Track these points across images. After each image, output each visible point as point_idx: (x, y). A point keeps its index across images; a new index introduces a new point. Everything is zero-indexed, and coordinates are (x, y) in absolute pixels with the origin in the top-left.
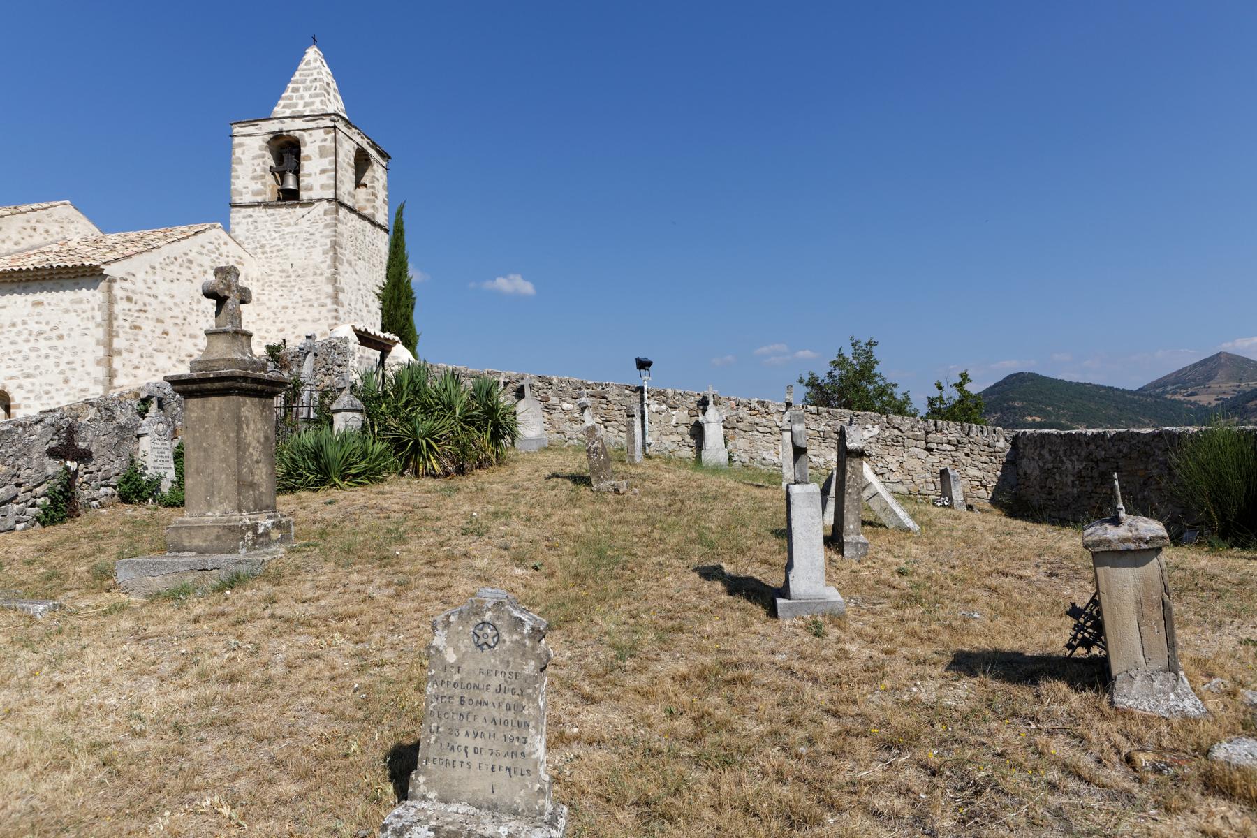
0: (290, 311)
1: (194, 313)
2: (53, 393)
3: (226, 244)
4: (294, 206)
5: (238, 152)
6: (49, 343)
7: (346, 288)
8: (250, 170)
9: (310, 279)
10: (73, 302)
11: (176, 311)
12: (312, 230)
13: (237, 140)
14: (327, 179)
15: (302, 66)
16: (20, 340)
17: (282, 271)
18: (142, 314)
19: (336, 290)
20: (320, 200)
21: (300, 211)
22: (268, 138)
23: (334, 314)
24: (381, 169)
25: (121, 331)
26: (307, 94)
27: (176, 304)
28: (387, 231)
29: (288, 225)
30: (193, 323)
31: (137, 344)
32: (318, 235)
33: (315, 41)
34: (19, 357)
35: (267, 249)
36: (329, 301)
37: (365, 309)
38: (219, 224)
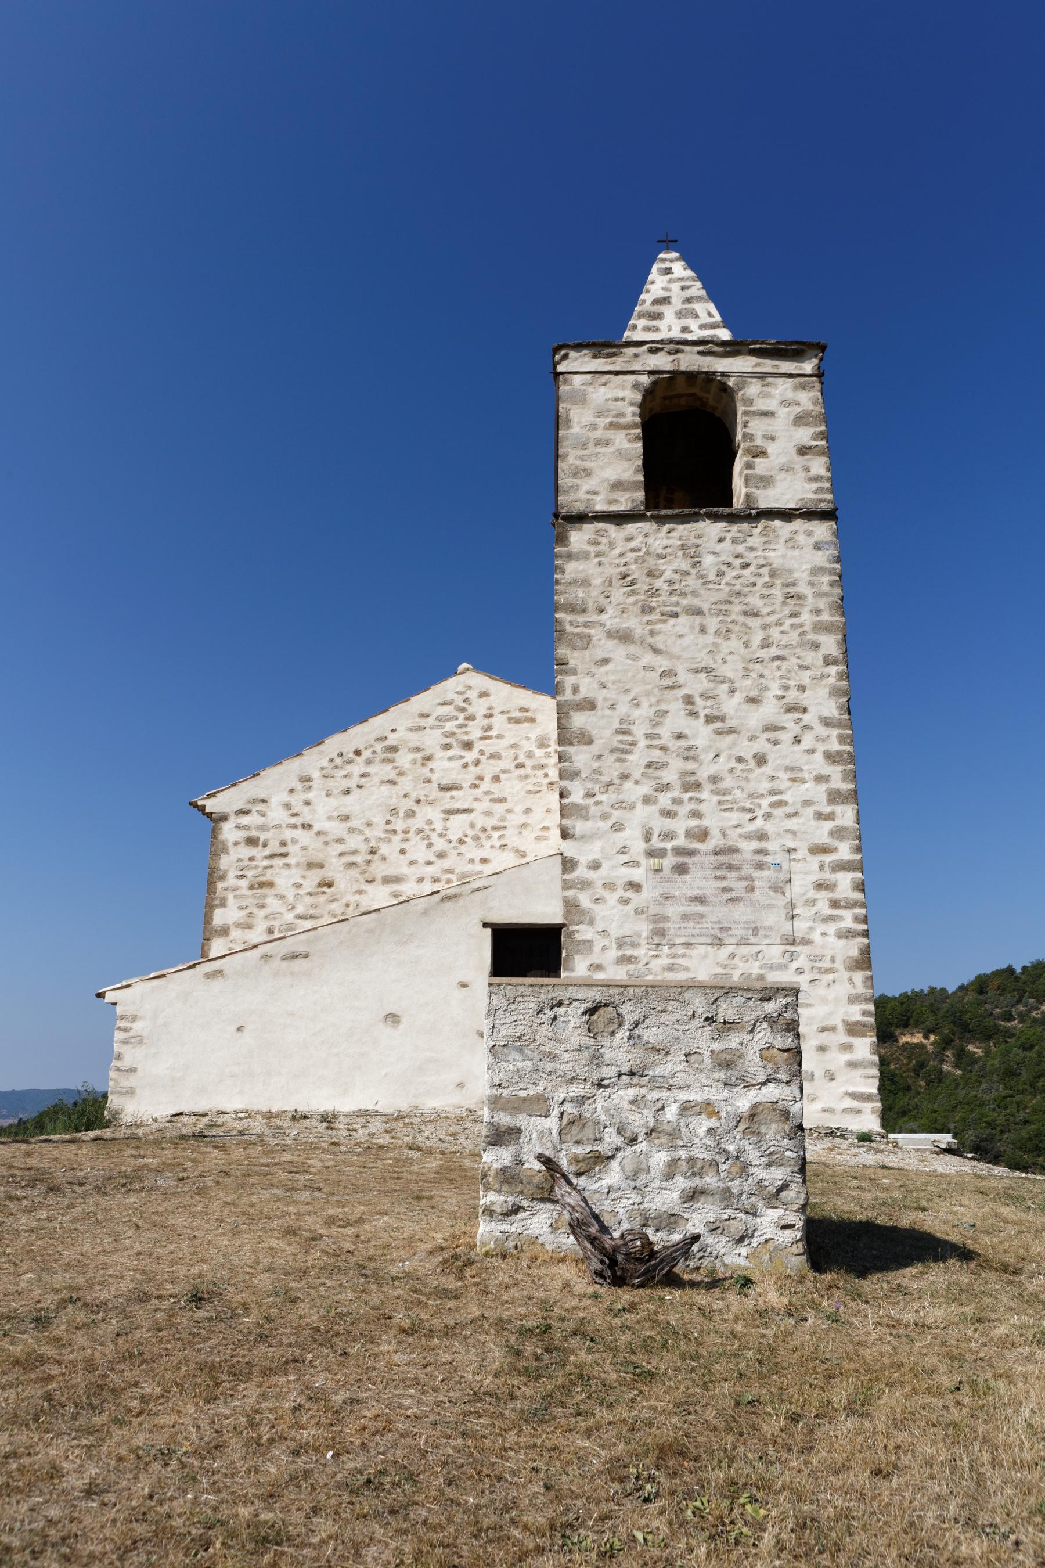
1: (396, 839)
3: (484, 694)
7: (600, 696)
11: (354, 842)
18: (278, 862)
24: (783, 388)
25: (230, 896)
27: (352, 830)
31: (262, 913)
33: (668, 244)
37: (701, 734)
38: (465, 665)
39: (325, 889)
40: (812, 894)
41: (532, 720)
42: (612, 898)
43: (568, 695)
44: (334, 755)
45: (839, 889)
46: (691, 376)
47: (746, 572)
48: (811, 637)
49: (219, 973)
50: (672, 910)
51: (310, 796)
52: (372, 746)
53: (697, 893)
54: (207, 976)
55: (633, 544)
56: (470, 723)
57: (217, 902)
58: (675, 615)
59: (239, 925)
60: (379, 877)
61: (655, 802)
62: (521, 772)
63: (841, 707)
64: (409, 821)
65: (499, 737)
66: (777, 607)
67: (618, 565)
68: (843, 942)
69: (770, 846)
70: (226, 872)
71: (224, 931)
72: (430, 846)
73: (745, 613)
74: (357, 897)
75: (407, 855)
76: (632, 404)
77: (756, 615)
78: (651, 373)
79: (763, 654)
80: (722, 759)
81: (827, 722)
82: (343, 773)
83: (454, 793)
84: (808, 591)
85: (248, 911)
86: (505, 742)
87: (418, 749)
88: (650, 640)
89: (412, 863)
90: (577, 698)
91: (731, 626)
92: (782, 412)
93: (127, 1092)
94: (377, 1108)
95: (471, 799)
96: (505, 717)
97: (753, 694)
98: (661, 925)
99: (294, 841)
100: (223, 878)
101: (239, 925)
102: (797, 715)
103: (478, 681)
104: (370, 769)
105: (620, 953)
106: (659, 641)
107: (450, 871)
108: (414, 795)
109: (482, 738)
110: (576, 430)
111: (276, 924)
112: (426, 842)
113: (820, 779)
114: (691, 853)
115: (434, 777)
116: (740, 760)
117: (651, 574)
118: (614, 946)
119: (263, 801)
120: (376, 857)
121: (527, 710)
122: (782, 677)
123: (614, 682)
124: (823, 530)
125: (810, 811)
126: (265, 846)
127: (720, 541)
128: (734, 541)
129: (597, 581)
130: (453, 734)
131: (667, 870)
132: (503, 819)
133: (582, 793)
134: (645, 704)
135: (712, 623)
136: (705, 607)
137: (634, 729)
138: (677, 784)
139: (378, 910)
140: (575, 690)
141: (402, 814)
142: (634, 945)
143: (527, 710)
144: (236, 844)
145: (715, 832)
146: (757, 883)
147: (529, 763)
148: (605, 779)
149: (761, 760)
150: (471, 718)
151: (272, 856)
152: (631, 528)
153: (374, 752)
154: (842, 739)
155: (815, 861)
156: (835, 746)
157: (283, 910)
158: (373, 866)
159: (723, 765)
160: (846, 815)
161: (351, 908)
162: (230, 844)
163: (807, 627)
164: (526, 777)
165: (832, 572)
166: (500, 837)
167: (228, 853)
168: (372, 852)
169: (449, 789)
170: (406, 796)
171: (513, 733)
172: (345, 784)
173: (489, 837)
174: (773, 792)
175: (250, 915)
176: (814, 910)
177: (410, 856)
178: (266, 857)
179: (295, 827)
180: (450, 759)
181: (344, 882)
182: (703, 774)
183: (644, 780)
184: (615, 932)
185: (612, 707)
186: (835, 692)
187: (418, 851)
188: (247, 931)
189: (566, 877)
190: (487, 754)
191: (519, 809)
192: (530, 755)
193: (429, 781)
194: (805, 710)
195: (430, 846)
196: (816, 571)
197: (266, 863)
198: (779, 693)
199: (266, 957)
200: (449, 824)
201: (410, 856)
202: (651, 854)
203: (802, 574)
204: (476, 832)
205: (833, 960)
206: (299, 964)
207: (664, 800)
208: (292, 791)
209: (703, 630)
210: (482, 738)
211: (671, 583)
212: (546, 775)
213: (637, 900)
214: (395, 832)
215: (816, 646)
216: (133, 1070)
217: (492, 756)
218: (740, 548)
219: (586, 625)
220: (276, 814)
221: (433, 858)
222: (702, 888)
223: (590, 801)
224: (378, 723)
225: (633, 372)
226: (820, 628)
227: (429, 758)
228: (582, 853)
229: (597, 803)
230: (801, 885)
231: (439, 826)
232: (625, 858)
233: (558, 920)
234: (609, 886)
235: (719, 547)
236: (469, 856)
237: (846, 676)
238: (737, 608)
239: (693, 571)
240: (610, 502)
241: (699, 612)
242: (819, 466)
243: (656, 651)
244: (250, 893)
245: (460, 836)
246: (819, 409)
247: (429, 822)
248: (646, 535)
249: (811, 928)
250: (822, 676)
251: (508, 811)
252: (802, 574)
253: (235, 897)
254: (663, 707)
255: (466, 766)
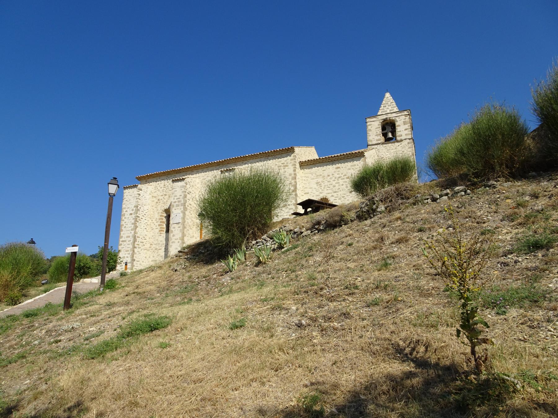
2: (346, 197)
4: (394, 142)
5: (369, 127)
6: (343, 180)
8: (375, 132)
10: (351, 166)
12: (403, 150)
13: (368, 124)
15: (385, 99)
16: (331, 180)
21: (397, 144)
22: (381, 121)
26: (390, 107)
33: (387, 91)
34: (331, 186)
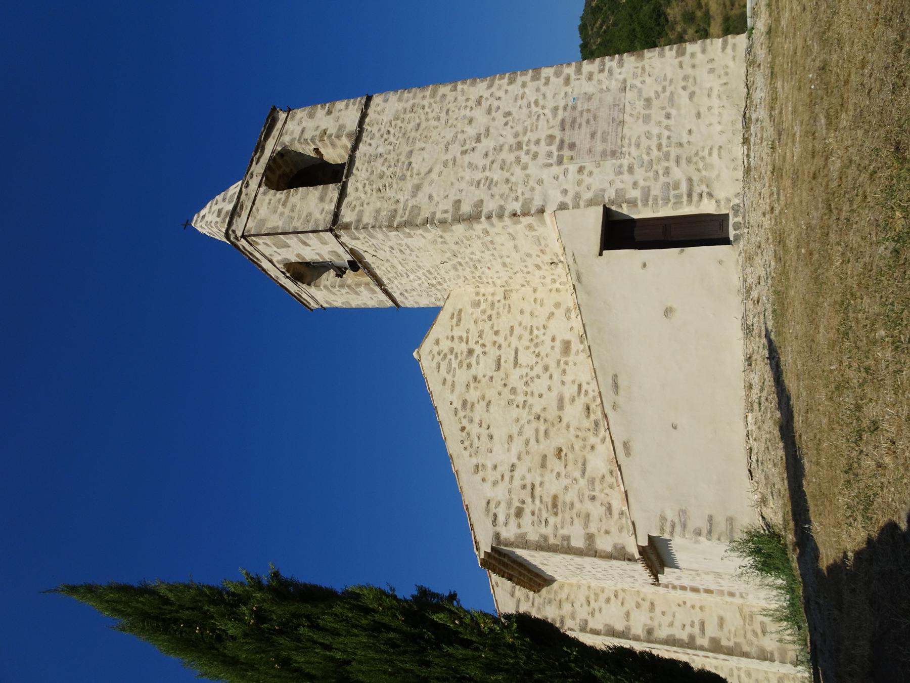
0: (508, 260)
1: (530, 400)
3: (437, 342)
7: (452, 198)
9: (455, 248)
11: (529, 432)
12: (387, 249)
13: (325, 305)
14: (312, 239)
17: (456, 270)
18: (537, 493)
19: (459, 219)
20: (342, 244)
21: (368, 259)
22: (304, 286)
23: (494, 220)
24: (290, 125)
25: (562, 532)
27: (520, 433)
28: (369, 99)
29: (393, 267)
30: (543, 402)
31: (578, 505)
32: (389, 243)
35: (434, 282)
36: (478, 228)
37: (488, 144)
38: (415, 354)
39: (563, 454)
40: (594, 82)
41: (460, 311)
42: (587, 180)
43: (449, 216)
44: (462, 446)
45: (592, 70)
46: (269, 168)
47: (392, 131)
48: (438, 99)
49: (625, 444)
50: (599, 147)
51: (489, 465)
52: (460, 419)
53: (588, 136)
54: (628, 453)
55: (360, 187)
56: (455, 351)
57: (565, 543)
58: (410, 163)
59: (586, 525)
60: (558, 413)
61: (527, 164)
62: (494, 317)
63: (482, 81)
64: (518, 391)
65: (468, 331)
66: (416, 115)
67: (372, 194)
68: (625, 65)
69: (562, 104)
70: (541, 536)
71: (590, 538)
72: (538, 377)
73: (417, 130)
74: (571, 429)
75: (543, 392)
76: (275, 195)
77: (419, 125)
78: (260, 186)
79: (443, 121)
80: (504, 133)
81: (490, 86)
82: (476, 440)
83: (502, 361)
84: (411, 102)
85: (575, 517)
86: (472, 328)
87: (468, 386)
88: (422, 175)
89: (549, 389)
90: (451, 210)
91: (423, 136)
92: (304, 124)
93: (731, 524)
94: (740, 317)
95: (508, 349)
96: (455, 328)
97: (466, 121)
98: (608, 153)
99: (523, 478)
100: (545, 538)
101: (586, 525)
102: (484, 100)
103: (428, 345)
104: (476, 420)
105: (626, 173)
106: (424, 171)
107: (559, 362)
108: (500, 388)
109: (467, 343)
110: (280, 224)
111: (587, 493)
112: (535, 379)
113: (524, 85)
114: (562, 142)
115: (489, 374)
116: (506, 124)
117: (381, 177)
118: (621, 176)
119: (488, 503)
120: (542, 415)
121: (453, 315)
122: (459, 109)
123: (445, 191)
124: (377, 99)
125: (543, 89)
126: (523, 502)
127: (370, 145)
128: (372, 138)
129: (379, 204)
130: (461, 362)
131: (572, 153)
132: (525, 328)
133: (515, 203)
134: (461, 174)
135: (419, 145)
136: (408, 149)
137: (477, 178)
138: (517, 153)
139: (584, 325)
140: (446, 212)
141: (513, 397)
142: (621, 166)
143: (453, 315)
144: (519, 526)
145: (550, 132)
146: (585, 107)
147: (489, 312)
148: (507, 191)
149: (508, 114)
150: (452, 350)
151: (533, 496)
152: (350, 189)
153: (465, 417)
154: (501, 78)
155: (573, 83)
156: (506, 81)
157: (576, 487)
158: (549, 418)
159: (508, 133)
160: (547, 72)
161: (579, 434)
162: (519, 531)
163: (432, 101)
164: (498, 314)
165: (402, 93)
166: (538, 329)
167: (526, 534)
168: (538, 418)
169: (499, 364)
170: (500, 394)
171: (467, 322)
172: (484, 438)
173: (537, 337)
174: (529, 106)
175: (578, 515)
176: (604, 80)
177: (544, 391)
178: (533, 501)
179: (512, 477)
180: (478, 363)
181: (559, 439)
182: (512, 141)
183: (511, 171)
184: (612, 176)
185: (461, 191)
186: (473, 84)
187: (539, 386)
188: (591, 518)
189: (571, 206)
190: (479, 339)
191: (519, 318)
192: (484, 312)
193: (492, 378)
194: (481, 97)
195: (538, 377)
196: (400, 100)
197: (537, 501)
198: (468, 109)
199: (615, 407)
200: (524, 364)
201: (544, 391)
202: (560, 162)
203: (400, 106)
204: (532, 345)
205: (637, 67)
206: (622, 382)
207: (525, 159)
208: (484, 480)
209: (423, 149)
210: (467, 343)
211: (390, 166)
212: (499, 301)
213: (589, 166)
214: (525, 402)
215: (444, 96)
216: (710, 519)
217: (481, 336)
218: (377, 135)
219: (404, 210)
220: (500, 493)
221: (548, 374)
222: (586, 135)
223: (521, 198)
224: (444, 414)
225: (256, 196)
226: (433, 95)
227: (475, 378)
228: (556, 197)
229: (523, 194)
230: (590, 88)
231: (524, 371)
232: (561, 177)
233: (601, 209)
234: (579, 183)
235: (374, 145)
236: (549, 350)
237: (464, 83)
238: (413, 134)
239: (385, 156)
240: (331, 201)
241: (411, 152)
242: (340, 105)
243: (430, 171)
244: (560, 515)
245: (534, 356)
246: (308, 109)
247: (521, 377)
248: (357, 181)
249: (616, 80)
250: (463, 91)
251: (520, 324)
252: (400, 106)
253: (562, 528)
254: (466, 164)
255: (484, 353)
